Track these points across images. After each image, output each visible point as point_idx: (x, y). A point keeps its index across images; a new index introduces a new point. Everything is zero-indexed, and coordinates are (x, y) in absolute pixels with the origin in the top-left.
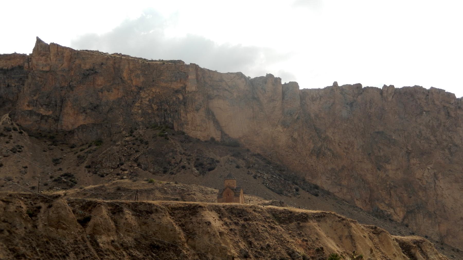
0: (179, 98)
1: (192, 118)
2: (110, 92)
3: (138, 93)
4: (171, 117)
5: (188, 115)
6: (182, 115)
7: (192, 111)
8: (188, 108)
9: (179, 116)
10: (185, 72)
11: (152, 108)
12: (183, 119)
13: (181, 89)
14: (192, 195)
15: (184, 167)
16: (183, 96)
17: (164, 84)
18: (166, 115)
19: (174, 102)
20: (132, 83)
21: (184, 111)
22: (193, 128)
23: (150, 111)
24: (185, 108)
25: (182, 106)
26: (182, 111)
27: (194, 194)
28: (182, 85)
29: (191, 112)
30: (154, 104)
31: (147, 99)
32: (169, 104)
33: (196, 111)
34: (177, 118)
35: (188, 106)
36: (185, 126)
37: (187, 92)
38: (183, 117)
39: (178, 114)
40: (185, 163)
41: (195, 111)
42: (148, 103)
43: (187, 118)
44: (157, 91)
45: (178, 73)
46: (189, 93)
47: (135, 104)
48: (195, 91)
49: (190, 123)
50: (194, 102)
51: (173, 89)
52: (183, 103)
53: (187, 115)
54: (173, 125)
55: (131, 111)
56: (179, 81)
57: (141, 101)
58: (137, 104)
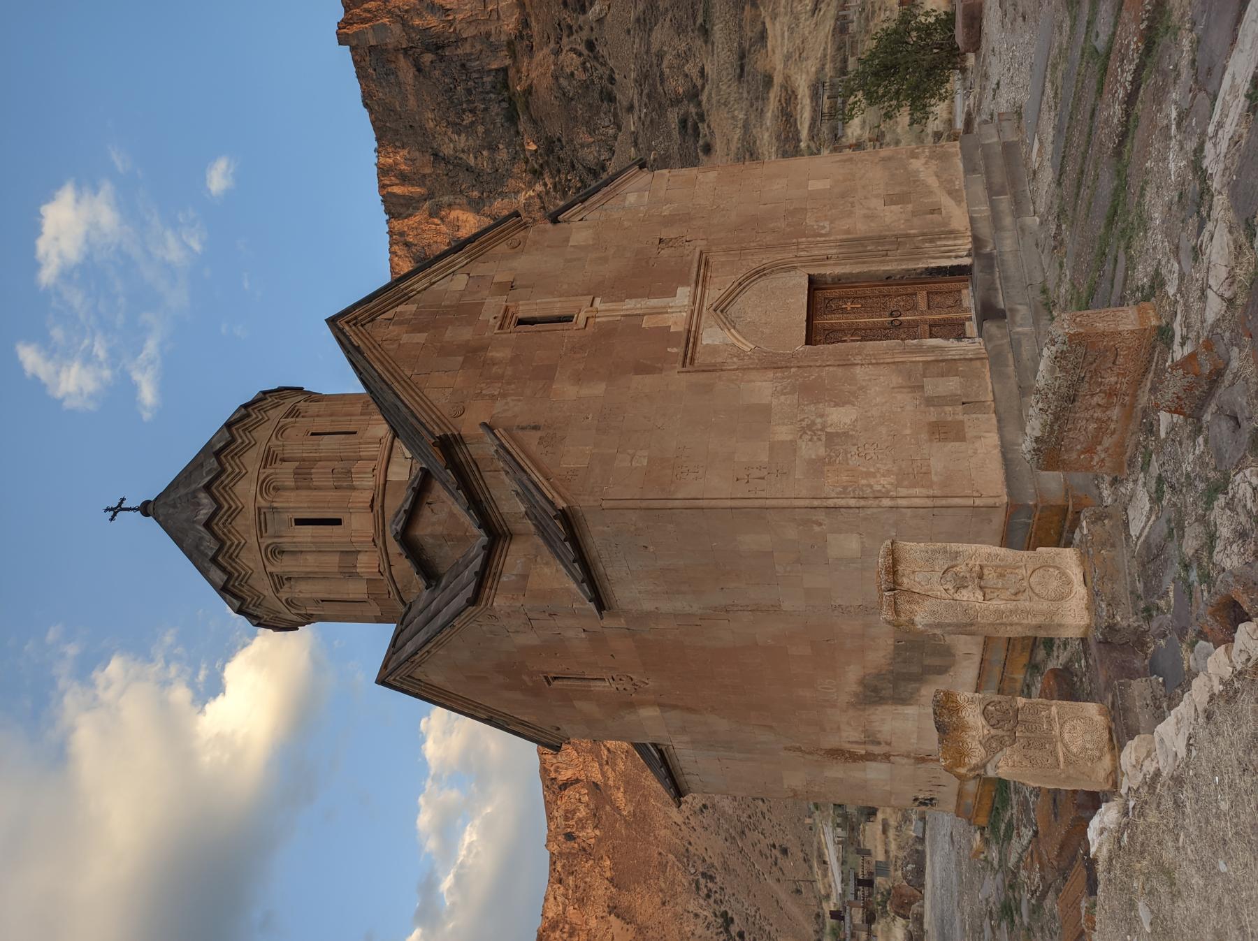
0: (432, 62)
1: (470, 23)
2: (460, 223)
3: (445, 160)
4: (482, 78)
5: (464, 36)
6: (468, 52)
7: (452, 25)
8: (447, 38)
9: (473, 57)
10: (367, 51)
11: (472, 123)
12: (479, 47)
13: (411, 59)
14: (664, 66)
15: (590, 45)
16: (422, 53)
17: (412, 102)
18: (480, 90)
19: (444, 74)
20: (430, 175)
21: (457, 47)
22: (495, 16)
23: (481, 129)
24: (449, 46)
25: (447, 54)
26: (459, 51)
27: (660, 56)
28: (401, 57)
29: (455, 29)
30: (463, 120)
31: (455, 137)
32: (452, 86)
33: (448, 15)
34: (478, 62)
35: (442, 39)
36: (492, 39)
37: (411, 45)
38: (473, 46)
39: (468, 61)
40: (579, 40)
41: (451, 18)
42: (463, 135)
43: (474, 37)
44: (430, 115)
45: (375, 70)
46: (410, 39)
47: (471, 167)
48: (403, 24)
49: (483, 29)
50: (428, 24)
51: (415, 76)
52: (440, 51)
53: (466, 38)
54: (497, 70)
55: (489, 174)
56: (393, 66)
57: (463, 151)
58: (472, 161)
